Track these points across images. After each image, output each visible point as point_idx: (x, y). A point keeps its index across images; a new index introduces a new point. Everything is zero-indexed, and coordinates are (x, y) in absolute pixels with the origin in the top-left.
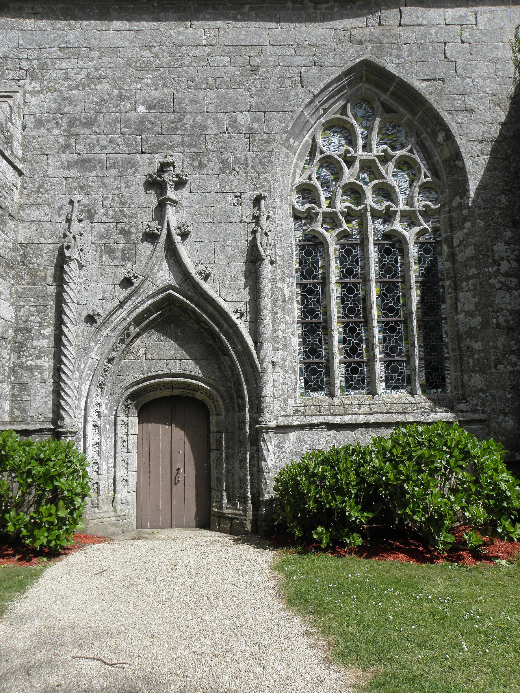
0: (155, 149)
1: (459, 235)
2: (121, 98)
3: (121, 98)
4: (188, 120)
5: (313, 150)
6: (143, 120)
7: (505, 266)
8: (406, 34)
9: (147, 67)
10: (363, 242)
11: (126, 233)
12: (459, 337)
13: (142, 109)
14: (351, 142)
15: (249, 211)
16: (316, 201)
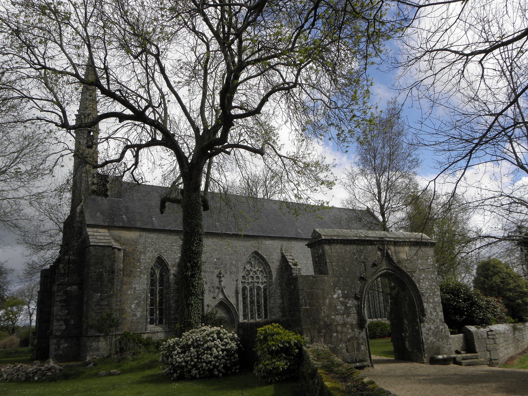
0: (218, 269)
1: (271, 288)
2: (211, 257)
3: (211, 257)
4: (224, 262)
5: (245, 268)
6: (216, 262)
7: (278, 294)
8: (263, 246)
9: (216, 250)
10: (254, 287)
11: (213, 287)
12: (270, 308)
13: (215, 260)
14: (252, 266)
15: (235, 282)
16: (245, 279)
